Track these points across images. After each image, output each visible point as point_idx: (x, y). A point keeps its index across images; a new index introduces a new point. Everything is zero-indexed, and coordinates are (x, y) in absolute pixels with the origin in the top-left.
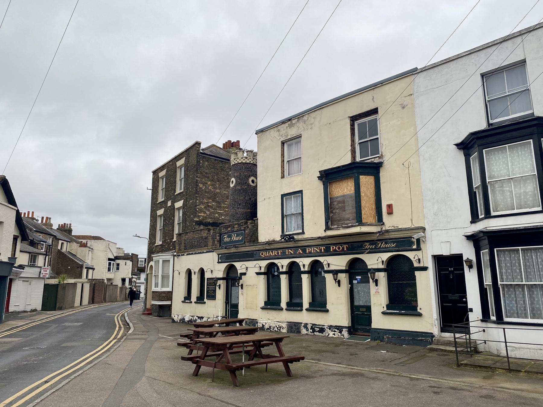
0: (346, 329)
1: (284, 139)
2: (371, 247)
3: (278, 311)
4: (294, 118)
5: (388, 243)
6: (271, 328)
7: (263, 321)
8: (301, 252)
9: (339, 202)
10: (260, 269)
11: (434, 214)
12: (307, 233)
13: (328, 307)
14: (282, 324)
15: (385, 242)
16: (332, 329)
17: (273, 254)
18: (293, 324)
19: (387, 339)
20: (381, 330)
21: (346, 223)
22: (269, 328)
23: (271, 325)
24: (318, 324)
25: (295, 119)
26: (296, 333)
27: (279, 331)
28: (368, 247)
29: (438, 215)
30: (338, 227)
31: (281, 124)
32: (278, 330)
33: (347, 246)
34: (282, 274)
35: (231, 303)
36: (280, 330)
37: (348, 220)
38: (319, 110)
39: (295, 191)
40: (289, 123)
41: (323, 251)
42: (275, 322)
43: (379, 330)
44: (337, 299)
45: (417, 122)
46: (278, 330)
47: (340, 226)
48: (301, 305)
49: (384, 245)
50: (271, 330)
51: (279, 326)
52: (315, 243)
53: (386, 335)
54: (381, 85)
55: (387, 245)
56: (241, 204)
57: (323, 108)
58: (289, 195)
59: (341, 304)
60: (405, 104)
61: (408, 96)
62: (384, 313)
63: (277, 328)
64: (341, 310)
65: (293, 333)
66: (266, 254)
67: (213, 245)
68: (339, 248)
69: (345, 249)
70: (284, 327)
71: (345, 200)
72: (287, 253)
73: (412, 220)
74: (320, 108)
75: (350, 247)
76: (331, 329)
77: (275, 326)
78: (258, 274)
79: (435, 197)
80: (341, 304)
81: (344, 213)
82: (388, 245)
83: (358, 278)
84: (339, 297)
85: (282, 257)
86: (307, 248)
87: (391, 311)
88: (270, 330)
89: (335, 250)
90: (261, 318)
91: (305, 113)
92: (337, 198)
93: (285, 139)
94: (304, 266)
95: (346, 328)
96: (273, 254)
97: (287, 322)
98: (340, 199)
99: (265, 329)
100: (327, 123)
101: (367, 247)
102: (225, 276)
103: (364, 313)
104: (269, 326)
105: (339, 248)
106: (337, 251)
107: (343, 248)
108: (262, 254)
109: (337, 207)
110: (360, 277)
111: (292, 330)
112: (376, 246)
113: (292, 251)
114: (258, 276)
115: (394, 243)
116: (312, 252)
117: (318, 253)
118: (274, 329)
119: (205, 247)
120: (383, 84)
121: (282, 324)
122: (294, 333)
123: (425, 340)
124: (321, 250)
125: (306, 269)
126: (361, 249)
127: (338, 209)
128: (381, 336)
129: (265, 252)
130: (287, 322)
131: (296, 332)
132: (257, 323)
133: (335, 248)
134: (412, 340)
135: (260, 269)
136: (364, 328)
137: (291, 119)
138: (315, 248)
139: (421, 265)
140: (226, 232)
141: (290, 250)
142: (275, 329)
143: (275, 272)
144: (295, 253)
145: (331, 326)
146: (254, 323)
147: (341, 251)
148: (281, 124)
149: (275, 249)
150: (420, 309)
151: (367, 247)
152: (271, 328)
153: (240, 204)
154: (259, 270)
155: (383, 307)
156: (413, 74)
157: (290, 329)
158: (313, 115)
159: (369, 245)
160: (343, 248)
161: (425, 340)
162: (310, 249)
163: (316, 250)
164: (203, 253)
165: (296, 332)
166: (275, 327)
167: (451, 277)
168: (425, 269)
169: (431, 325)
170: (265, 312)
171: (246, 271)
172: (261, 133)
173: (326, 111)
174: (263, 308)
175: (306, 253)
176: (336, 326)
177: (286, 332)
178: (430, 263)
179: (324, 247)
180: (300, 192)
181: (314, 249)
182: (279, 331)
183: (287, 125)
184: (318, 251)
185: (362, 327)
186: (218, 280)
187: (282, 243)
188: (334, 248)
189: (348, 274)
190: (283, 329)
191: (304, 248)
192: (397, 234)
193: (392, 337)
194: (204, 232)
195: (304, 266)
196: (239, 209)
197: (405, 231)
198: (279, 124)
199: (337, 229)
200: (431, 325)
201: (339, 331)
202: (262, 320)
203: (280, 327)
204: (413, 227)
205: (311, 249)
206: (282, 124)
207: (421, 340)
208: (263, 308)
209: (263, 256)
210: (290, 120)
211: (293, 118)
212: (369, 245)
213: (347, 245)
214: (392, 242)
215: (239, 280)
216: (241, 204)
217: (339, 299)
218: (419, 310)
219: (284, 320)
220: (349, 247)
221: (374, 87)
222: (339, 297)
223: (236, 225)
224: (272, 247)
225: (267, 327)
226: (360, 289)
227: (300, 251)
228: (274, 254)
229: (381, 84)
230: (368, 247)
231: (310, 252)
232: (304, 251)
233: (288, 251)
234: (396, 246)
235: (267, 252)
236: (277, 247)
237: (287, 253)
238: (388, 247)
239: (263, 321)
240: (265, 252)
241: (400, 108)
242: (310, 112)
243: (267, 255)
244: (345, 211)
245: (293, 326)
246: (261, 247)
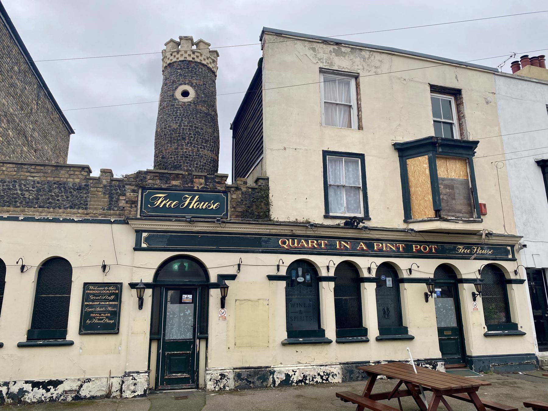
0: (442, 362)
1: (325, 66)
2: (465, 251)
3: (320, 347)
4: (347, 46)
5: (484, 248)
6: (306, 379)
7: (287, 368)
8: (365, 248)
9: (446, 186)
10: (278, 270)
11: (524, 224)
12: (373, 220)
13: (411, 332)
14: (330, 369)
15: (481, 247)
16: (422, 364)
17: (308, 243)
18: (354, 365)
19: (494, 368)
20: (485, 358)
21: (457, 215)
22: (301, 379)
23: (307, 373)
24: (398, 360)
25: (346, 47)
26: (361, 380)
27: (324, 381)
28: (462, 251)
29: (527, 225)
30: (457, 219)
31: (321, 41)
32: (323, 380)
33: (436, 246)
34: (460, 283)
35: (164, 339)
36: (327, 380)
37: (460, 212)
38: (387, 55)
39: (350, 152)
40: (336, 47)
41: (401, 250)
42: (315, 367)
43: (482, 358)
44: (425, 320)
45: (500, 124)
46: (323, 380)
47: (459, 219)
48: (364, 332)
49: (480, 250)
50: (307, 382)
51: (324, 372)
52: (392, 237)
53: (492, 363)
54: (465, 67)
55: (484, 251)
56: (208, 141)
57: (383, 53)
58: (337, 154)
59: (431, 327)
60: (489, 100)
61: (491, 94)
62: (486, 335)
63: (322, 377)
64: (427, 336)
65: (354, 381)
66: (293, 244)
67: (109, 209)
68: (425, 249)
69: (434, 251)
70: (335, 372)
71: (454, 186)
72: (338, 247)
73: (504, 226)
74: (390, 52)
75: (440, 249)
76: (420, 365)
77: (316, 374)
78: (271, 278)
79: (523, 206)
80: (431, 327)
81: (454, 202)
82: (484, 252)
83: (438, 291)
84: (427, 317)
85: (328, 252)
86: (374, 242)
87: (495, 332)
88: (305, 383)
89: (419, 251)
90: (281, 364)
91: (366, 47)
92: (443, 181)
93: (326, 67)
94: (369, 269)
95: (441, 360)
96: (308, 243)
97: (340, 364)
98: (447, 182)
99: (292, 382)
100: (401, 78)
101: (460, 250)
102: (460, 285)
103: (450, 337)
104: (302, 375)
105: (425, 249)
106: (423, 252)
107: (431, 249)
108: (284, 243)
109: (444, 192)
110: (440, 290)
111: (352, 376)
112: (471, 251)
113: (347, 244)
114: (271, 282)
115: (490, 249)
116: (384, 249)
117: (394, 251)
118: (313, 380)
119: (71, 207)
120: (468, 67)
121: (330, 369)
122: (357, 380)
123: (531, 363)
124: (398, 248)
125: (332, 274)
126: (454, 252)
127: (445, 195)
128: (486, 366)
129: (290, 240)
130: (340, 364)
131: (360, 378)
132: (273, 373)
133: (418, 248)
134: (518, 365)
135: (278, 270)
136: (451, 357)
137: (341, 44)
138: (388, 244)
139: (518, 277)
140: (163, 187)
141: (344, 241)
142: (315, 380)
143: (297, 276)
144: (353, 248)
145: (418, 360)
146: (264, 375)
147: (427, 253)
148: (321, 41)
149: (315, 237)
150: (521, 327)
151: (460, 250)
152: (308, 378)
153: (206, 141)
154: (409, 274)
155: (484, 328)
156: (494, 74)
157: (348, 374)
158: (378, 56)
159: (463, 248)
160: (431, 249)
161: (531, 363)
162: (381, 245)
163: (391, 248)
164: (73, 221)
165: (360, 378)
166: (317, 376)
167: (535, 292)
168: (521, 282)
169: (532, 344)
170: (291, 350)
171: (238, 271)
172: (275, 37)
173: (399, 63)
174: (284, 344)
175: (373, 250)
176: (425, 360)
177: (340, 381)
178: (523, 275)
179: (403, 245)
180: (360, 157)
181: (386, 246)
182: (324, 381)
183: (331, 48)
184: (394, 249)
185: (448, 357)
186: (144, 288)
187: (330, 229)
188: (417, 247)
189: (361, 283)
190: (335, 377)
191: (370, 243)
192: (498, 240)
193: (498, 365)
194: (70, 173)
195: (369, 269)
196: (204, 148)
197: (511, 238)
198: (316, 41)
199: (455, 221)
200: (532, 344)
201: (431, 366)
202: (282, 366)
203: (328, 375)
204: (506, 234)
205: (382, 245)
206: (321, 43)
207: (527, 363)
208: (284, 344)
209: (285, 246)
210: (338, 43)
211: (345, 44)
212: (463, 248)
213: (403, 244)
214: (488, 248)
216: (208, 141)
217: (427, 319)
218: (520, 329)
219: (334, 361)
220: (439, 248)
221: (458, 65)
222: (427, 317)
223: (202, 178)
224: (310, 233)
225: (295, 378)
226: (441, 306)
227: (363, 246)
228: (310, 246)
229: (466, 66)
230: (462, 251)
231: (381, 250)
232: (370, 246)
233: (340, 243)
234: (493, 254)
235: (296, 240)
236: (321, 234)
237: (338, 247)
238: (484, 254)
239: (287, 368)
240: (290, 240)
241: (484, 102)
242: (374, 50)
243: (296, 245)
244: (454, 199)
245: (354, 369)
246: (275, 230)
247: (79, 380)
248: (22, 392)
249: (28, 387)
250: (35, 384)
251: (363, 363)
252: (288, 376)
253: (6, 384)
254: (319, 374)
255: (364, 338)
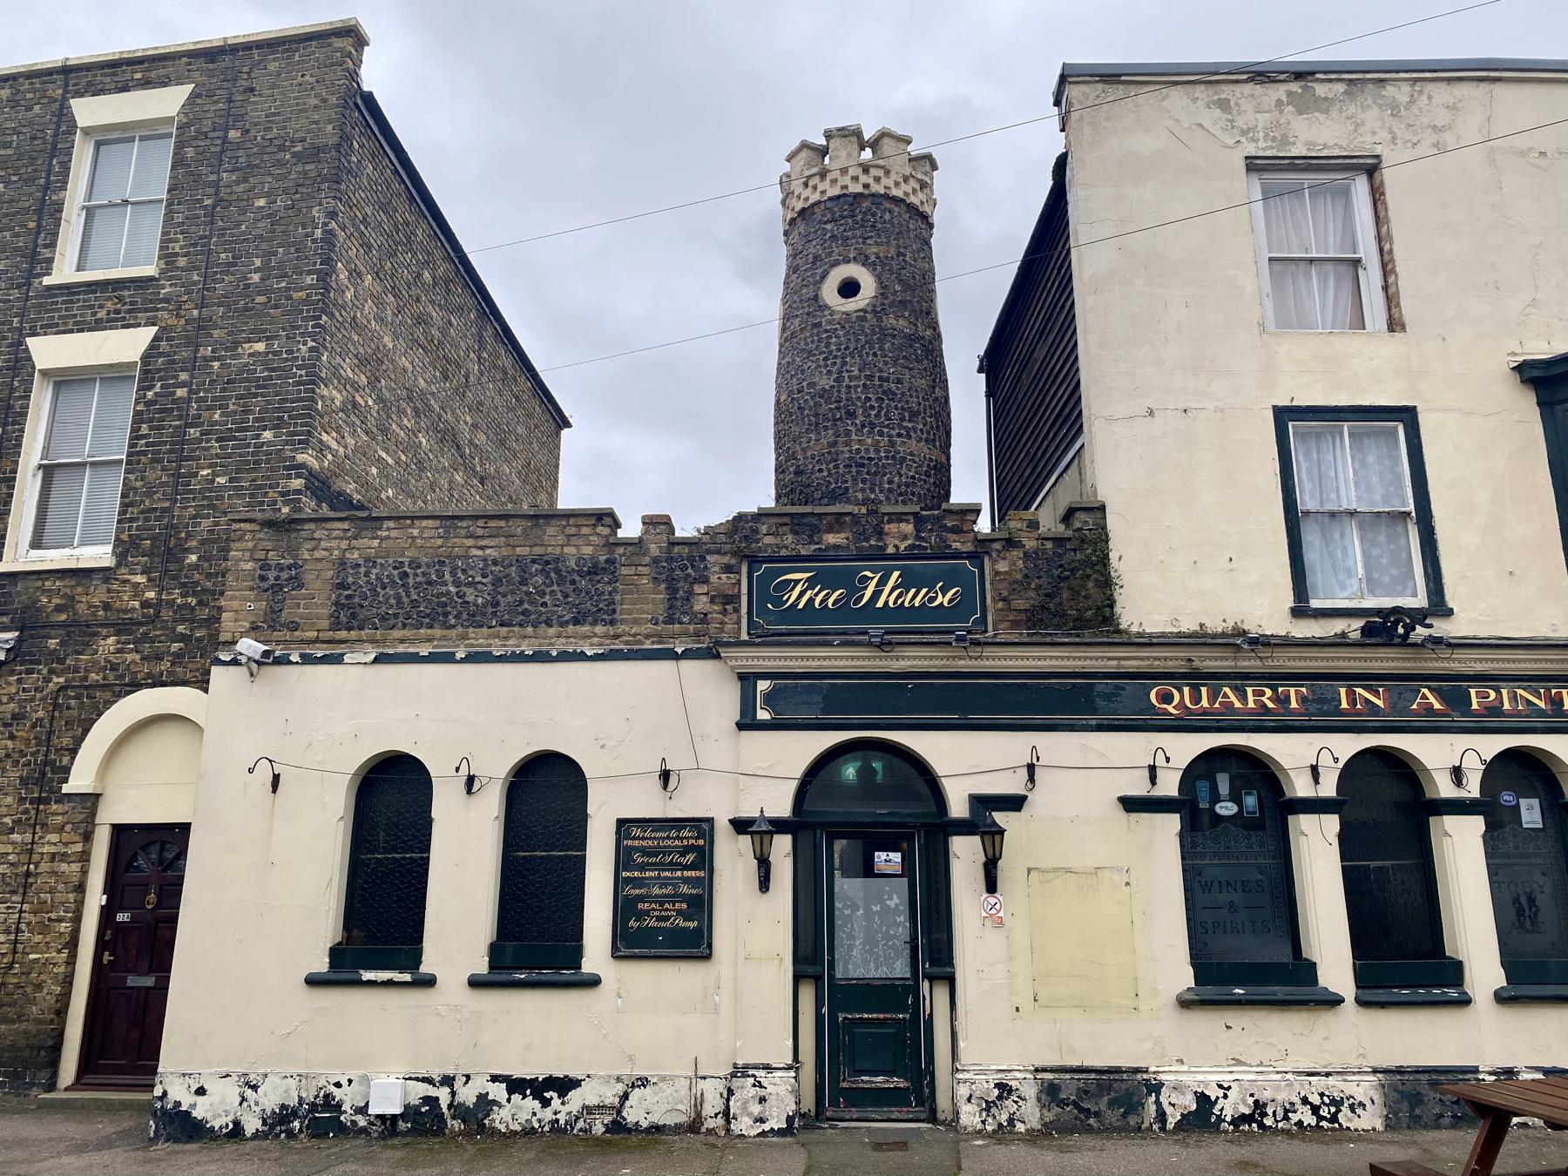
1: (1264, 149)
4: (1333, 76)
6: (1265, 1114)
8: (1437, 706)
10: (1153, 780)
14: (1341, 1085)
17: (1243, 698)
22: (1247, 1112)
23: (1265, 1096)
25: (1330, 81)
26: (1453, 1127)
27: (1324, 1124)
31: (1245, 77)
35: (832, 977)
36: (1334, 1119)
39: (1367, 403)
40: (1295, 87)
42: (1289, 1076)
48: (1453, 973)
50: (1268, 1122)
51: (1322, 1095)
58: (1321, 415)
63: (1315, 1110)
65: (1426, 1127)
66: (1196, 699)
67: (670, 620)
70: (1359, 1098)
72: (1344, 705)
77: (1297, 1100)
78: (1131, 805)
85: (1311, 724)
86: (1471, 687)
88: (1261, 1126)
90: (1181, 1061)
91: (1398, 72)
93: (1269, 153)
94: (1457, 774)
96: (1243, 698)
97: (1375, 1071)
99: (1220, 1119)
100: (1530, 149)
104: (1251, 1101)
108: (1166, 699)
111: (1417, 1111)
113: (1377, 694)
114: (1134, 816)
116: (1507, 706)
117: (1541, 713)
118: (1286, 1118)
119: (576, 622)
121: (1341, 1085)
122: (1438, 1127)
125: (1328, 789)
129: (1186, 690)
130: (1375, 1071)
131: (1446, 1121)
132: (1156, 1088)
135: (1153, 780)
137: (1313, 73)
138: (1520, 691)
141: (1363, 687)
142: (1294, 1118)
143: (1215, 798)
146: (1129, 1094)
148: (1245, 77)
152: (1270, 1111)
153: (914, 415)
157: (1405, 1106)
158: (1441, 94)
162: (1493, 695)
163: (1529, 702)
164: (581, 657)
165: (1446, 1121)
166: (1298, 1106)
170: (1208, 1023)
171: (1030, 786)
172: (1100, 86)
174: (1185, 1003)
182: (1324, 1124)
183: (1279, 91)
184: (1542, 705)
186: (771, 833)
191: (1453, 688)
195: (1457, 774)
196: (908, 436)
202: (1185, 1068)
203: (1337, 1103)
206: (1246, 81)
208: (1185, 1003)
209: (1170, 708)
210: (1301, 74)
215: (766, 838)
219: (1354, 1062)
223: (907, 521)
224: (1248, 664)
225: (1230, 1107)
227: (1432, 699)
231: (1495, 710)
235: (1204, 690)
237: (1344, 705)
239: (1200, 1077)
240: (1186, 690)
243: (1205, 703)
245: (1425, 1089)
246: (1134, 660)
247: (618, 1079)
248: (485, 1103)
249: (498, 1091)
250: (516, 1086)
251: (1457, 1072)
252: (1202, 1099)
253: (448, 1081)
254: (1305, 1101)
255: (1453, 993)
